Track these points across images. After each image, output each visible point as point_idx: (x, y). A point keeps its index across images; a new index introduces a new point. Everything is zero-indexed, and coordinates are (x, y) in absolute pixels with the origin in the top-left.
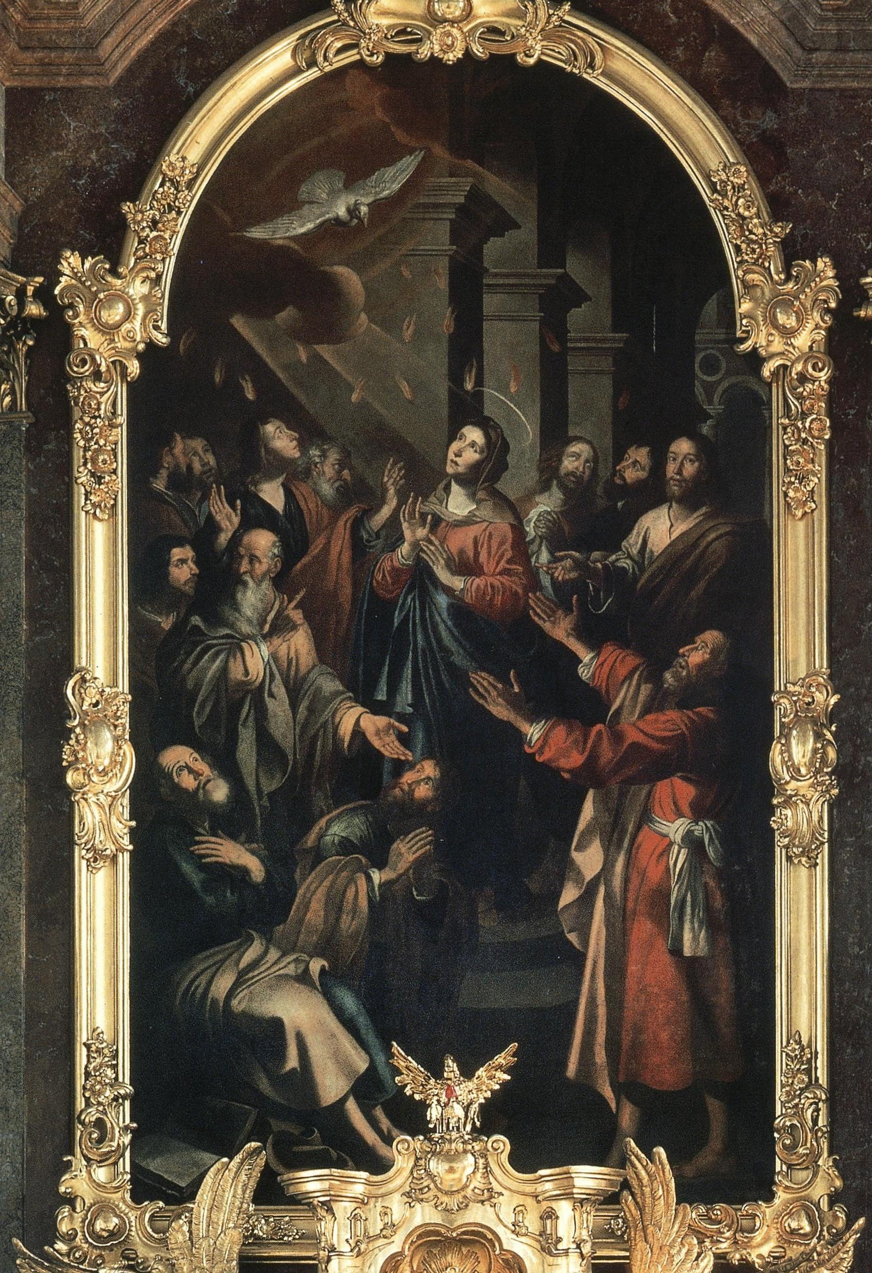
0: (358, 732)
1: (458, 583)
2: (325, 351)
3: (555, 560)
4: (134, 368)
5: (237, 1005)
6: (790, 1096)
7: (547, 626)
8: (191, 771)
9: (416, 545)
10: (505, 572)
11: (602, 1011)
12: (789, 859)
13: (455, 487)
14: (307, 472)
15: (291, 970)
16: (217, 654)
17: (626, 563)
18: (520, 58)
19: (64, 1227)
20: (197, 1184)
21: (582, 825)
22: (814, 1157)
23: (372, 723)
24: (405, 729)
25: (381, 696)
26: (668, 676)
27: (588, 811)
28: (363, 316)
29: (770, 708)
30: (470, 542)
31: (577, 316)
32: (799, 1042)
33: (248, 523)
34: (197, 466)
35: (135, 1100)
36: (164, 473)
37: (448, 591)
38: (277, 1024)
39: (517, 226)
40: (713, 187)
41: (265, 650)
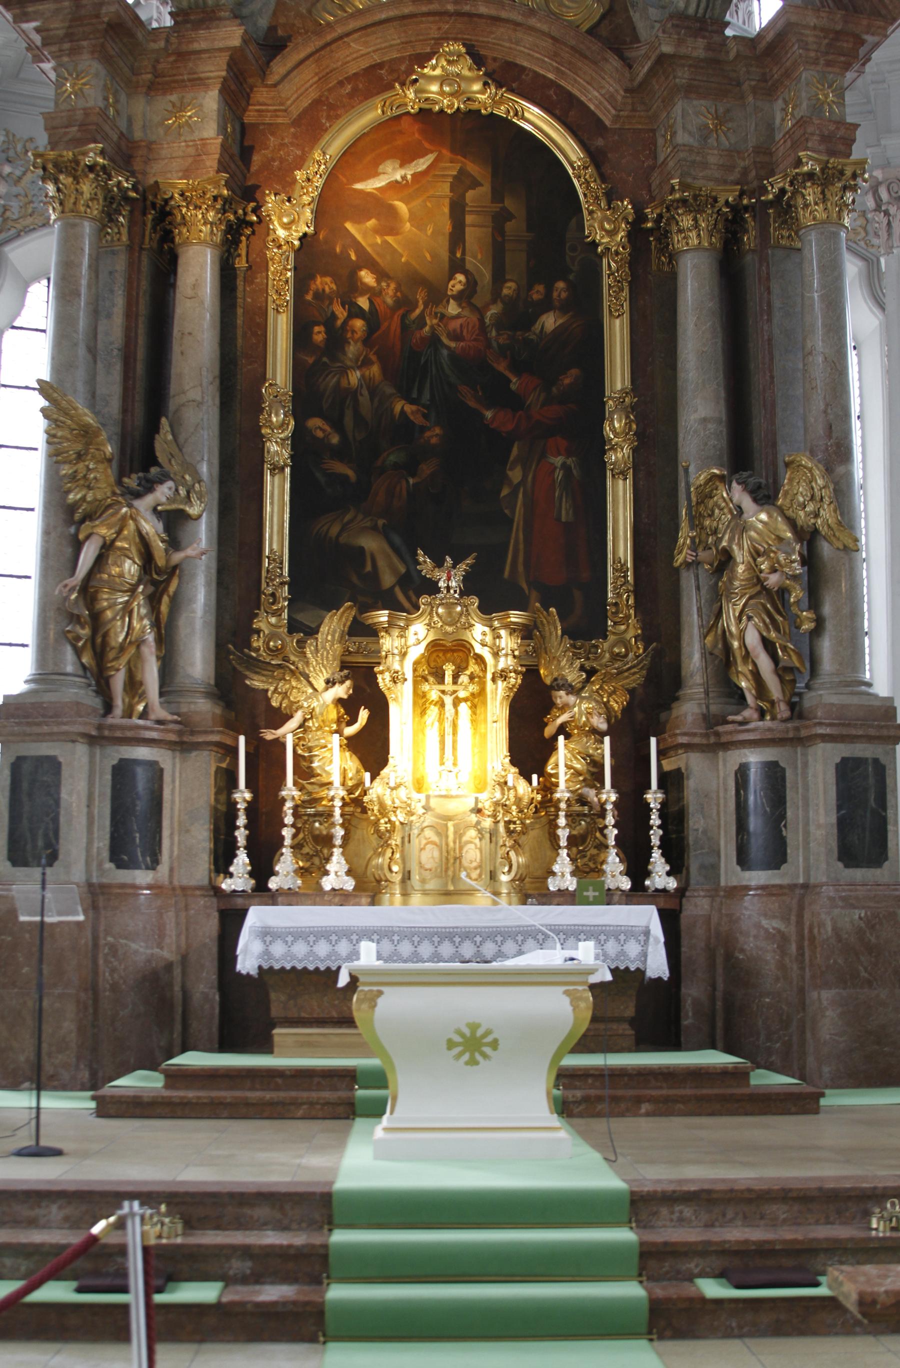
0: (402, 411)
1: (453, 345)
2: (389, 239)
3: (498, 334)
4: (297, 243)
5: (343, 540)
6: (615, 588)
7: (495, 365)
8: (321, 429)
9: (432, 327)
10: (475, 340)
11: (521, 546)
12: (613, 476)
13: (451, 301)
14: (380, 292)
15: (368, 524)
16: (334, 376)
17: (533, 337)
18: (483, 112)
19: (255, 645)
20: (319, 627)
21: (512, 458)
22: (628, 617)
23: (409, 408)
24: (426, 411)
25: (415, 395)
26: (554, 390)
27: (515, 451)
28: (408, 225)
29: (603, 404)
30: (458, 326)
31: (509, 226)
32: (620, 562)
33: (351, 316)
34: (327, 289)
35: (290, 585)
36: (311, 292)
37: (448, 348)
38: (362, 549)
39: (481, 185)
40: (573, 168)
41: (358, 373)
